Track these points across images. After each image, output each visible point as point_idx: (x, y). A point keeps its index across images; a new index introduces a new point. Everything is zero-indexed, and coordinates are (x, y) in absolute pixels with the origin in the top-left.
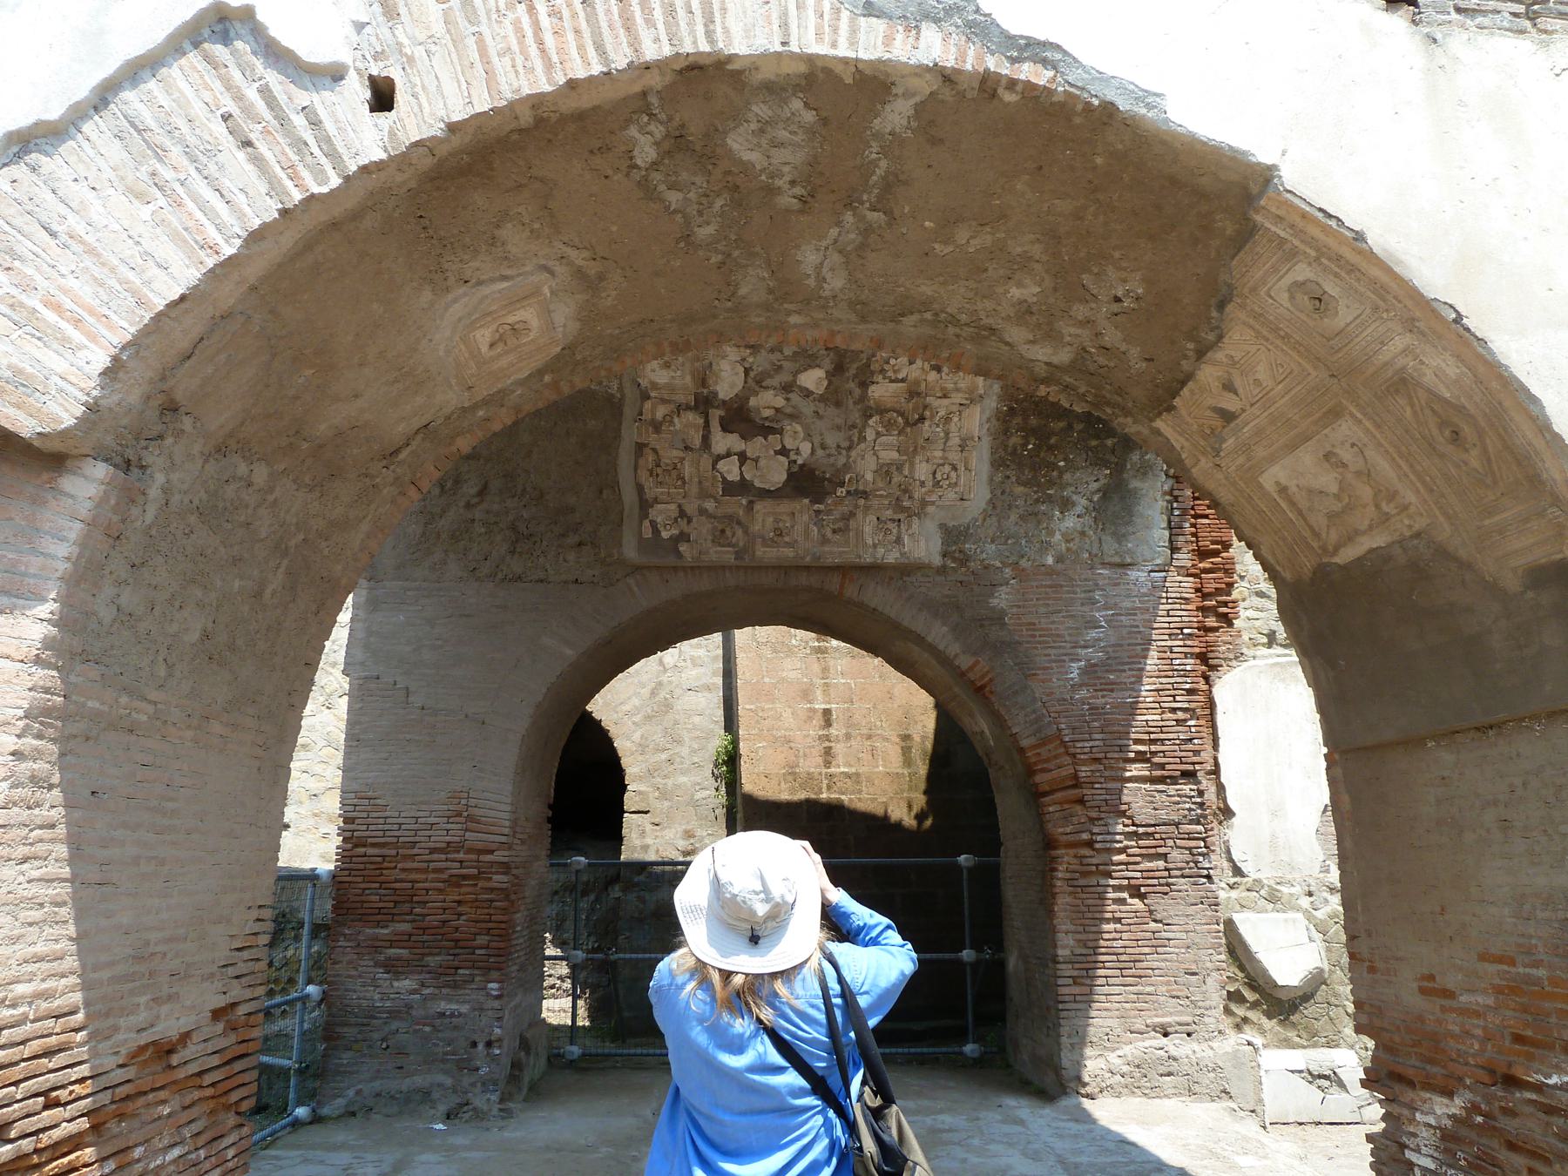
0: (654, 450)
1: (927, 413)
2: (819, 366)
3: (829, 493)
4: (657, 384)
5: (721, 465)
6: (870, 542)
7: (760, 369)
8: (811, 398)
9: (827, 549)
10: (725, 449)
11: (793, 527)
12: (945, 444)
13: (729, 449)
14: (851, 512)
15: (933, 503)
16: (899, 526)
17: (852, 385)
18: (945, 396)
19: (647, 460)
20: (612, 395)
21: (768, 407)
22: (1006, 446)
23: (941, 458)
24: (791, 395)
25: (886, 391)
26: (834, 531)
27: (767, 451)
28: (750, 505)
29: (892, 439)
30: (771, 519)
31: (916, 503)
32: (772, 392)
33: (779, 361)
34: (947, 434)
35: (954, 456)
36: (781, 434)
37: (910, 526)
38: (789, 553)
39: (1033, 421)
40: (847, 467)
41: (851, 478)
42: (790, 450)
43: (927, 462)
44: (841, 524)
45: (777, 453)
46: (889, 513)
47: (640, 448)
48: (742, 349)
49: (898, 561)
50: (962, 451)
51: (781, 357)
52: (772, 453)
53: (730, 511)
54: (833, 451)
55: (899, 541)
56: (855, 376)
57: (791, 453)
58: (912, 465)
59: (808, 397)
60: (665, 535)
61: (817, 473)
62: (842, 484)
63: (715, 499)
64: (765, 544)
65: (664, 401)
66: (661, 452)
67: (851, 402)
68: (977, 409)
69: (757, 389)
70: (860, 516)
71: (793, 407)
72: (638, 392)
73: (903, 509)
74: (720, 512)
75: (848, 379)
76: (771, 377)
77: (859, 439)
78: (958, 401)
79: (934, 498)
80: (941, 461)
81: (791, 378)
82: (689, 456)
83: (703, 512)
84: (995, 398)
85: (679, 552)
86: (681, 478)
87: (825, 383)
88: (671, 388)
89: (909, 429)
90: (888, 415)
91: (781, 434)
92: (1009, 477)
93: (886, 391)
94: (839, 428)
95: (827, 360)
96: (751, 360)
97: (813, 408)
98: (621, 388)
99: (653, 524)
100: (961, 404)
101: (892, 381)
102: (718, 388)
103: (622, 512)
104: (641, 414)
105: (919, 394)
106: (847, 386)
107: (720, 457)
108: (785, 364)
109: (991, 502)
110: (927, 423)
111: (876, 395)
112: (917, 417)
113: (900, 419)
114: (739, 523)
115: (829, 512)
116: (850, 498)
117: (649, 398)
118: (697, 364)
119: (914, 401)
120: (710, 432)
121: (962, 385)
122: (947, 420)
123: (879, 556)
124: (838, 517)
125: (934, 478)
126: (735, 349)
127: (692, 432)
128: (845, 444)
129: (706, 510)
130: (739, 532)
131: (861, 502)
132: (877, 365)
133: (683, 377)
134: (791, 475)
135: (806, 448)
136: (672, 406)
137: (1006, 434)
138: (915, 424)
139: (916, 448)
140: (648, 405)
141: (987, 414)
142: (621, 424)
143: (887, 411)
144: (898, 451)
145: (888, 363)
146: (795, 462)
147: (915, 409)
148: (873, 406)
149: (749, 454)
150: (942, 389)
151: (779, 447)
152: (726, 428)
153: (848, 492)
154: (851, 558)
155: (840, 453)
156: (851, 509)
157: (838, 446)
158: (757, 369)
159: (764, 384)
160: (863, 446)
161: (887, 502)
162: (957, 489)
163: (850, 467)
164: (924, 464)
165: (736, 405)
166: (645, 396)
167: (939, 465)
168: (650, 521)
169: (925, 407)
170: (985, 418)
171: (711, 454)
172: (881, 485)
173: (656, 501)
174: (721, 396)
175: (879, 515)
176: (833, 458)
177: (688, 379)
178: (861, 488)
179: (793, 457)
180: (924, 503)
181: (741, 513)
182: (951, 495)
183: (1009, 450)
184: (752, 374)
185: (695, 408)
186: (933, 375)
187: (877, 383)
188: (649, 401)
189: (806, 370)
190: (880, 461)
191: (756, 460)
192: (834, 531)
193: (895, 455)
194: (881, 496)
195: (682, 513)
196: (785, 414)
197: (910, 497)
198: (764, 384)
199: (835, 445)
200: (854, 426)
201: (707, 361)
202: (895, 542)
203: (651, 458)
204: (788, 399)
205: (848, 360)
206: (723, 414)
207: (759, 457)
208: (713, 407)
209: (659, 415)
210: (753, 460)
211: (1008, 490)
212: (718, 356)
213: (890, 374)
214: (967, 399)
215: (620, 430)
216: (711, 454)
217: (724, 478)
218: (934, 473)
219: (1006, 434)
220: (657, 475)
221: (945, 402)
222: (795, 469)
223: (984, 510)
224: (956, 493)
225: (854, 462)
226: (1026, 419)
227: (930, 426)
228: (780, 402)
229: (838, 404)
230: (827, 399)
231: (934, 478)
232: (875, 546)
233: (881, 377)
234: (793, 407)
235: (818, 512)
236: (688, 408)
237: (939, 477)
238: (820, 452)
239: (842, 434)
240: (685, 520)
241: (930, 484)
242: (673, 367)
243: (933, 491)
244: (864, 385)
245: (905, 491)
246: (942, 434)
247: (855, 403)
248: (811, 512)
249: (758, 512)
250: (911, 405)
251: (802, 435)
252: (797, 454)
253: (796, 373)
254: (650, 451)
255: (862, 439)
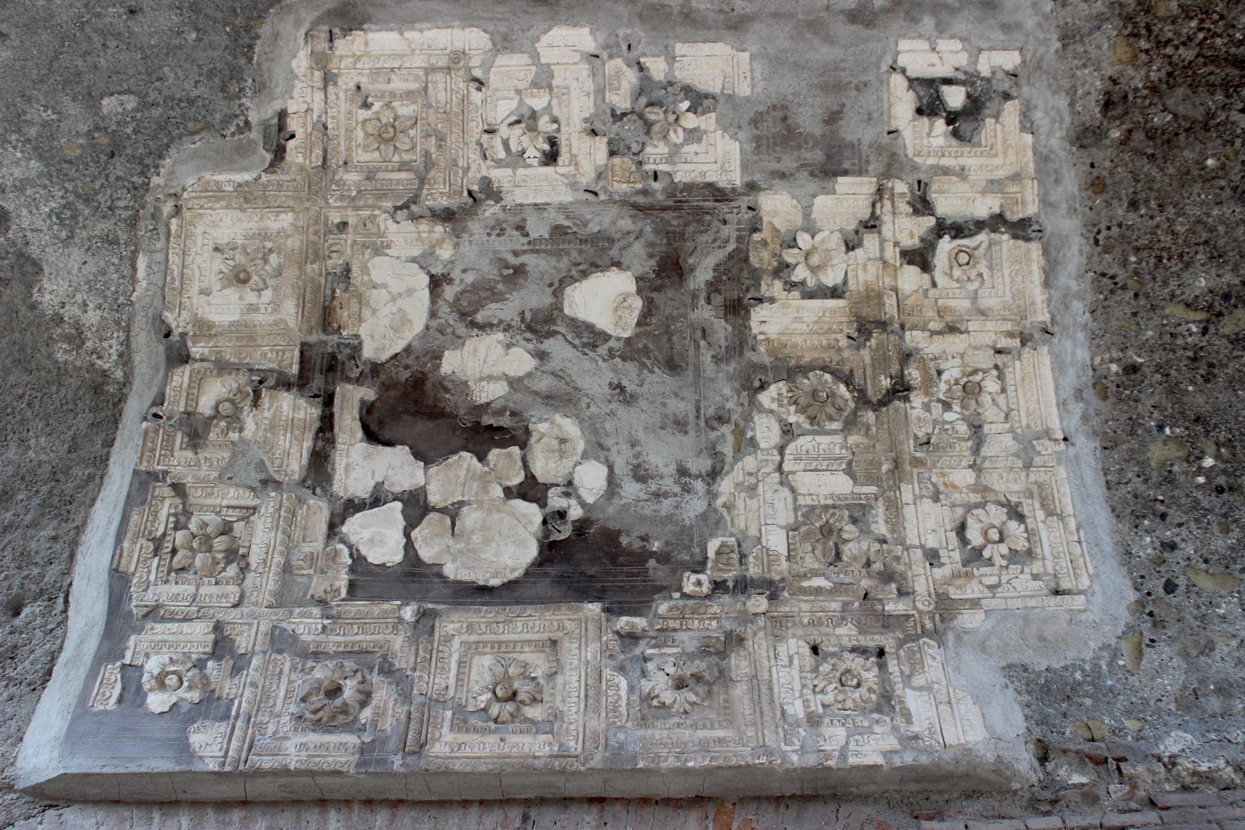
0: (179, 489)
1: (914, 374)
2: (618, 264)
3: (659, 589)
4: (210, 325)
5: (355, 527)
6: (796, 709)
7: (470, 278)
8: (603, 350)
9: (658, 733)
10: (372, 484)
11: (552, 676)
12: (976, 450)
13: (379, 485)
14: (728, 634)
15: (975, 604)
16: (882, 667)
17: (705, 313)
18: (952, 329)
19: (156, 515)
20: (104, 374)
21: (490, 378)
22: (1143, 464)
23: (975, 488)
24: (550, 345)
25: (796, 320)
26: (680, 684)
27: (486, 491)
28: (426, 618)
29: (829, 443)
30: (487, 660)
31: (924, 604)
32: (500, 336)
33: (516, 254)
34: (976, 428)
35: (1008, 484)
36: (523, 446)
37: (917, 664)
38: (537, 746)
39: (1197, 399)
40: (712, 521)
41: (723, 545)
42: (547, 487)
43: (936, 498)
44: (700, 665)
45: (509, 493)
46: (847, 633)
47: (144, 481)
48: (424, 226)
49: (897, 762)
50: (1028, 466)
51: (520, 242)
52: (498, 492)
53: (364, 639)
54: (669, 484)
55: (886, 702)
56: (713, 287)
57: (551, 493)
58: (894, 508)
59: (594, 346)
60: (157, 702)
61: (624, 541)
62: (699, 566)
63: (322, 602)
64: (462, 722)
65: (222, 367)
66: (195, 496)
67: (707, 357)
68: (1040, 361)
69: (462, 330)
70: (758, 643)
71: (553, 374)
72: (162, 348)
73: (887, 622)
74: (333, 641)
75: (695, 296)
76: (496, 297)
77: (738, 450)
78: (988, 339)
79: (972, 590)
80: (974, 498)
81: (549, 300)
82: (269, 503)
83: (280, 641)
84: (1080, 336)
85: (188, 746)
86: (233, 555)
87: (638, 303)
88: (244, 333)
89: (869, 416)
90: (806, 383)
91: (523, 446)
92: (1172, 547)
93: (796, 320)
94: (680, 425)
95: (638, 248)
96: (446, 253)
97: (609, 377)
98: (125, 358)
99: (131, 673)
100: (999, 352)
101: (810, 295)
102: (363, 331)
103: (53, 657)
104: (159, 400)
105: (883, 325)
106: (693, 316)
107: (353, 506)
108: (530, 260)
109: (1144, 607)
110: (917, 399)
111: (772, 330)
112: (886, 383)
113: (842, 389)
114: (387, 670)
115: (663, 637)
116: (726, 599)
117: (185, 359)
118: (312, 268)
119: (873, 342)
120: (332, 442)
121: (987, 301)
122: (971, 390)
123: (832, 746)
124: (691, 647)
125: (964, 541)
126: (408, 226)
127: (283, 441)
128: (701, 464)
129: (294, 637)
130: (383, 693)
131: (759, 603)
132: (765, 255)
133: (276, 305)
134: (550, 550)
135: (591, 479)
136: (243, 379)
137: (1132, 433)
138: (884, 403)
139: (897, 464)
140: (182, 376)
141: (1071, 379)
142: (109, 443)
143: (804, 370)
144: (849, 472)
145: (793, 243)
146: (562, 514)
147: (880, 362)
148: (767, 360)
149: (434, 498)
150: (940, 313)
151: (517, 479)
152: (372, 435)
153: (718, 586)
154: (743, 755)
155: (687, 489)
156: (728, 626)
157: (683, 472)
158: (463, 279)
159: (480, 317)
160: (749, 462)
161: (835, 605)
162: (1037, 567)
163: (719, 522)
164: (927, 504)
165: (404, 375)
166: (178, 356)
167: (969, 508)
168: (123, 666)
169: (906, 357)
170: (1068, 393)
171: (332, 498)
172: (810, 562)
173: (154, 613)
174: (368, 352)
175: (816, 637)
176: (666, 505)
177: (290, 308)
178: (753, 571)
179: (556, 501)
180: (945, 607)
181: (398, 642)
182: (1022, 582)
183: (1155, 477)
184: (449, 292)
185: (301, 383)
186: (910, 278)
187: (772, 300)
188: (187, 368)
189: (585, 274)
190: (801, 501)
191: (453, 512)
192: (680, 684)
193: (841, 484)
194: (818, 591)
195: (222, 645)
196: (536, 393)
197: (901, 593)
198: (480, 317)
199: (673, 467)
200: (721, 419)
201: (336, 262)
202: (879, 710)
203: (167, 508)
204: (541, 356)
205: (689, 245)
206: (368, 393)
207: (461, 504)
208: (349, 380)
209: (205, 405)
210: (443, 511)
211: (1181, 582)
212: (365, 246)
213: (800, 273)
214: (1010, 335)
215: (105, 460)
216: (332, 498)
217: (358, 560)
218: (961, 529)
219: (1132, 433)
220: (174, 551)
221: (955, 343)
222: (564, 532)
223: (1130, 628)
224: (1035, 577)
225: (728, 507)
226: (1173, 390)
227: (927, 407)
228: (520, 361)
229: (672, 366)
230: (646, 351)
231: (964, 541)
232: (813, 721)
233: (778, 285)
234: (553, 374)
235: (631, 638)
236: (284, 384)
237: (974, 536)
238: (631, 490)
239: (689, 439)
240: (227, 663)
241: (953, 557)
242: (255, 278)
243: (969, 576)
244: (736, 309)
245: (887, 576)
246: (963, 428)
247: (717, 360)
248: (608, 637)
249: (448, 639)
250: (866, 354)
251: (581, 446)
252: (567, 495)
253: (558, 288)
254: (167, 491)
255: (746, 444)
